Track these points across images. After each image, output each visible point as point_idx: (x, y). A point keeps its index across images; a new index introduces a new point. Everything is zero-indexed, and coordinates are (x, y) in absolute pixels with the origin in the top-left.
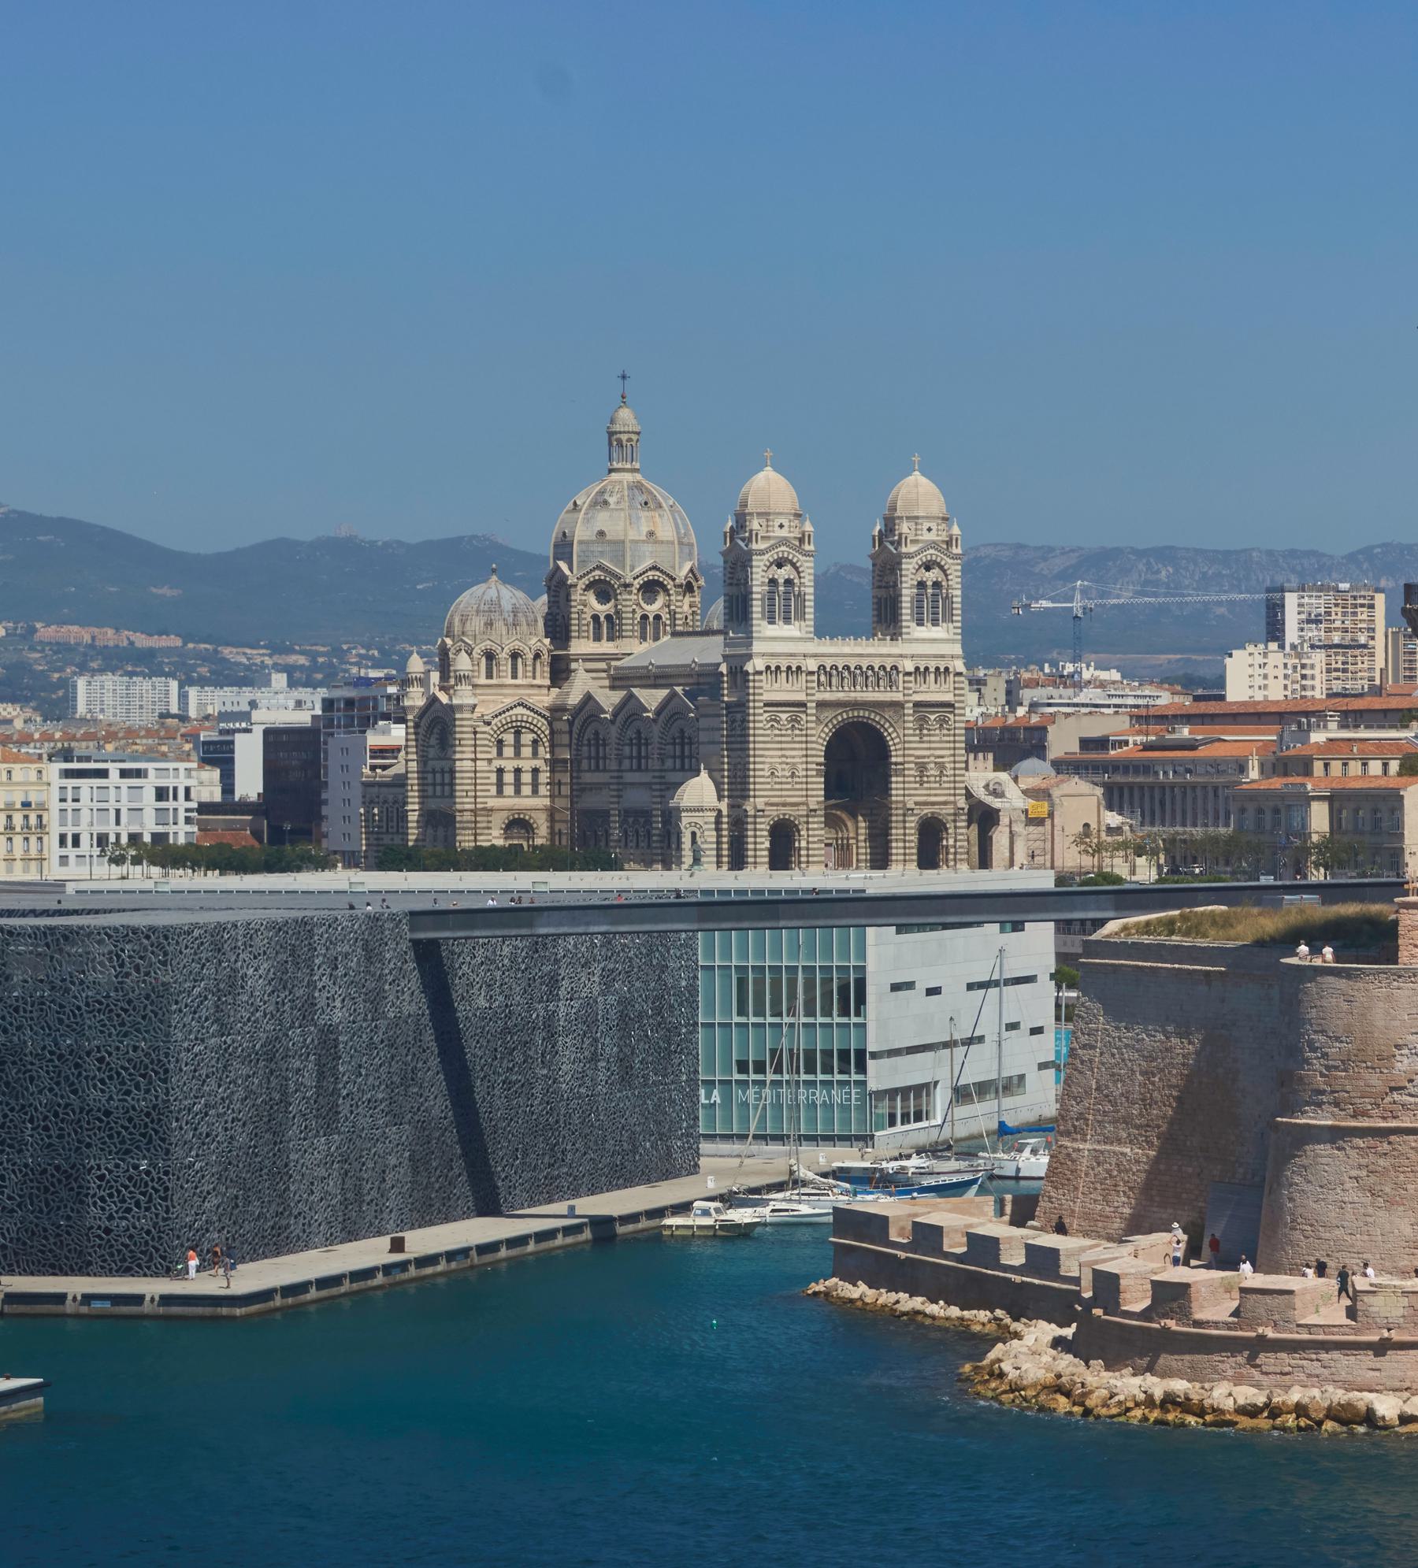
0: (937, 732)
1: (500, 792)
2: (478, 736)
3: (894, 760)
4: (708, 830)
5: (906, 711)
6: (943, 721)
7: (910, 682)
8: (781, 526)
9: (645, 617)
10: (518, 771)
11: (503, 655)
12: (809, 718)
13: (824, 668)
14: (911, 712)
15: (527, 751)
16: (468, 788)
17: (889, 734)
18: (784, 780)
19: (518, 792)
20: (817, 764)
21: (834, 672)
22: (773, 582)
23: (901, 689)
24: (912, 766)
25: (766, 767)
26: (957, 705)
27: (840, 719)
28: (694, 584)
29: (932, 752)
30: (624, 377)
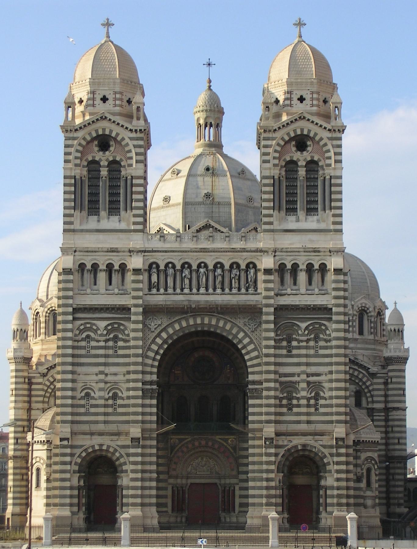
0: (312, 343)
2: (34, 387)
3: (251, 378)
5: (264, 318)
8: (104, 99)
13: (158, 266)
14: (272, 318)
17: (244, 347)
18: (102, 402)
23: (259, 291)
24: (272, 385)
25: (79, 385)
26: (334, 310)
27: (177, 327)
29: (303, 368)
30: (209, 64)
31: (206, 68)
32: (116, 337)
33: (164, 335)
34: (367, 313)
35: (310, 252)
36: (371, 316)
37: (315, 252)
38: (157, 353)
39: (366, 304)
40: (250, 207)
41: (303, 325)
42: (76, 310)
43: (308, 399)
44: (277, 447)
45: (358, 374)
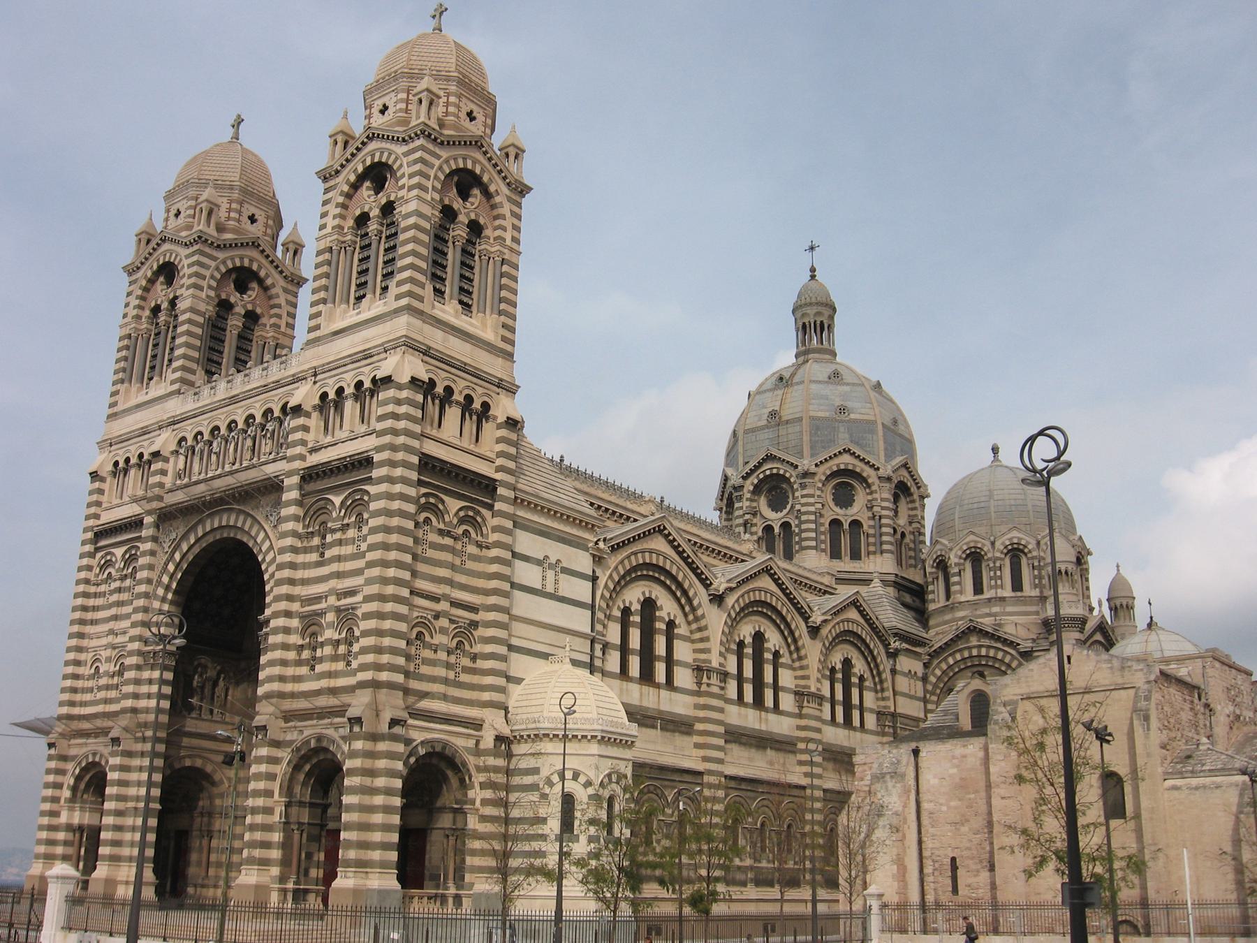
0: (351, 533)
6: (357, 506)
8: (178, 214)
9: (768, 529)
26: (377, 458)
29: (333, 583)
30: (812, 248)
31: (809, 254)
33: (177, 556)
34: (1026, 554)
35: (359, 361)
36: (1033, 558)
37: (366, 359)
38: (167, 588)
39: (1020, 539)
40: (842, 421)
41: (337, 500)
42: (99, 535)
43: (338, 642)
44: (276, 744)
45: (1004, 657)
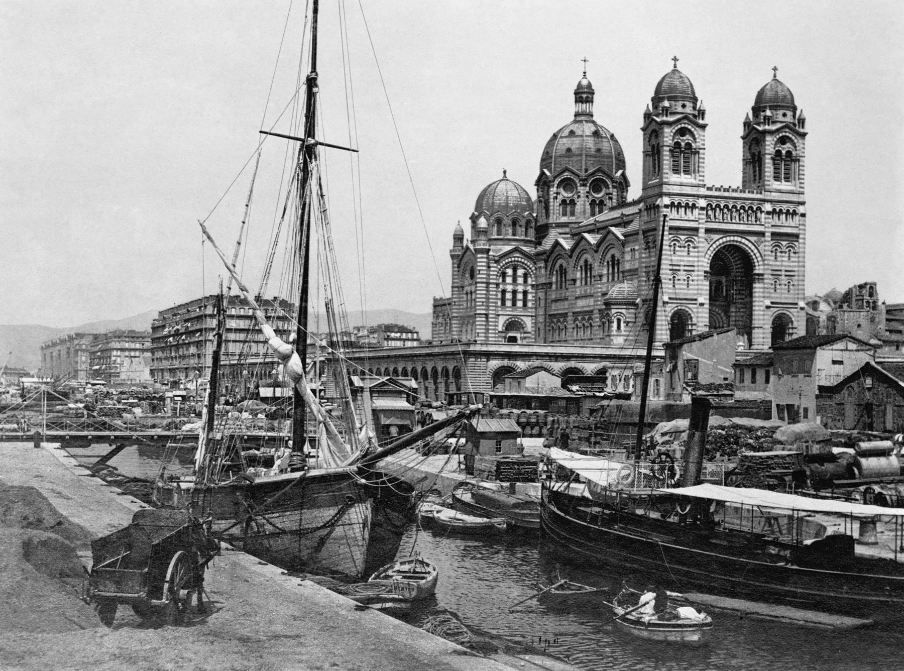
1: (503, 304)
4: (629, 318)
7: (769, 218)
10: (514, 292)
11: (507, 221)
12: (700, 240)
13: (711, 206)
14: (770, 239)
15: (520, 280)
16: (484, 300)
19: (514, 304)
20: (705, 272)
21: (718, 209)
22: (677, 144)
28: (624, 184)
30: (585, 61)
32: (689, 245)
